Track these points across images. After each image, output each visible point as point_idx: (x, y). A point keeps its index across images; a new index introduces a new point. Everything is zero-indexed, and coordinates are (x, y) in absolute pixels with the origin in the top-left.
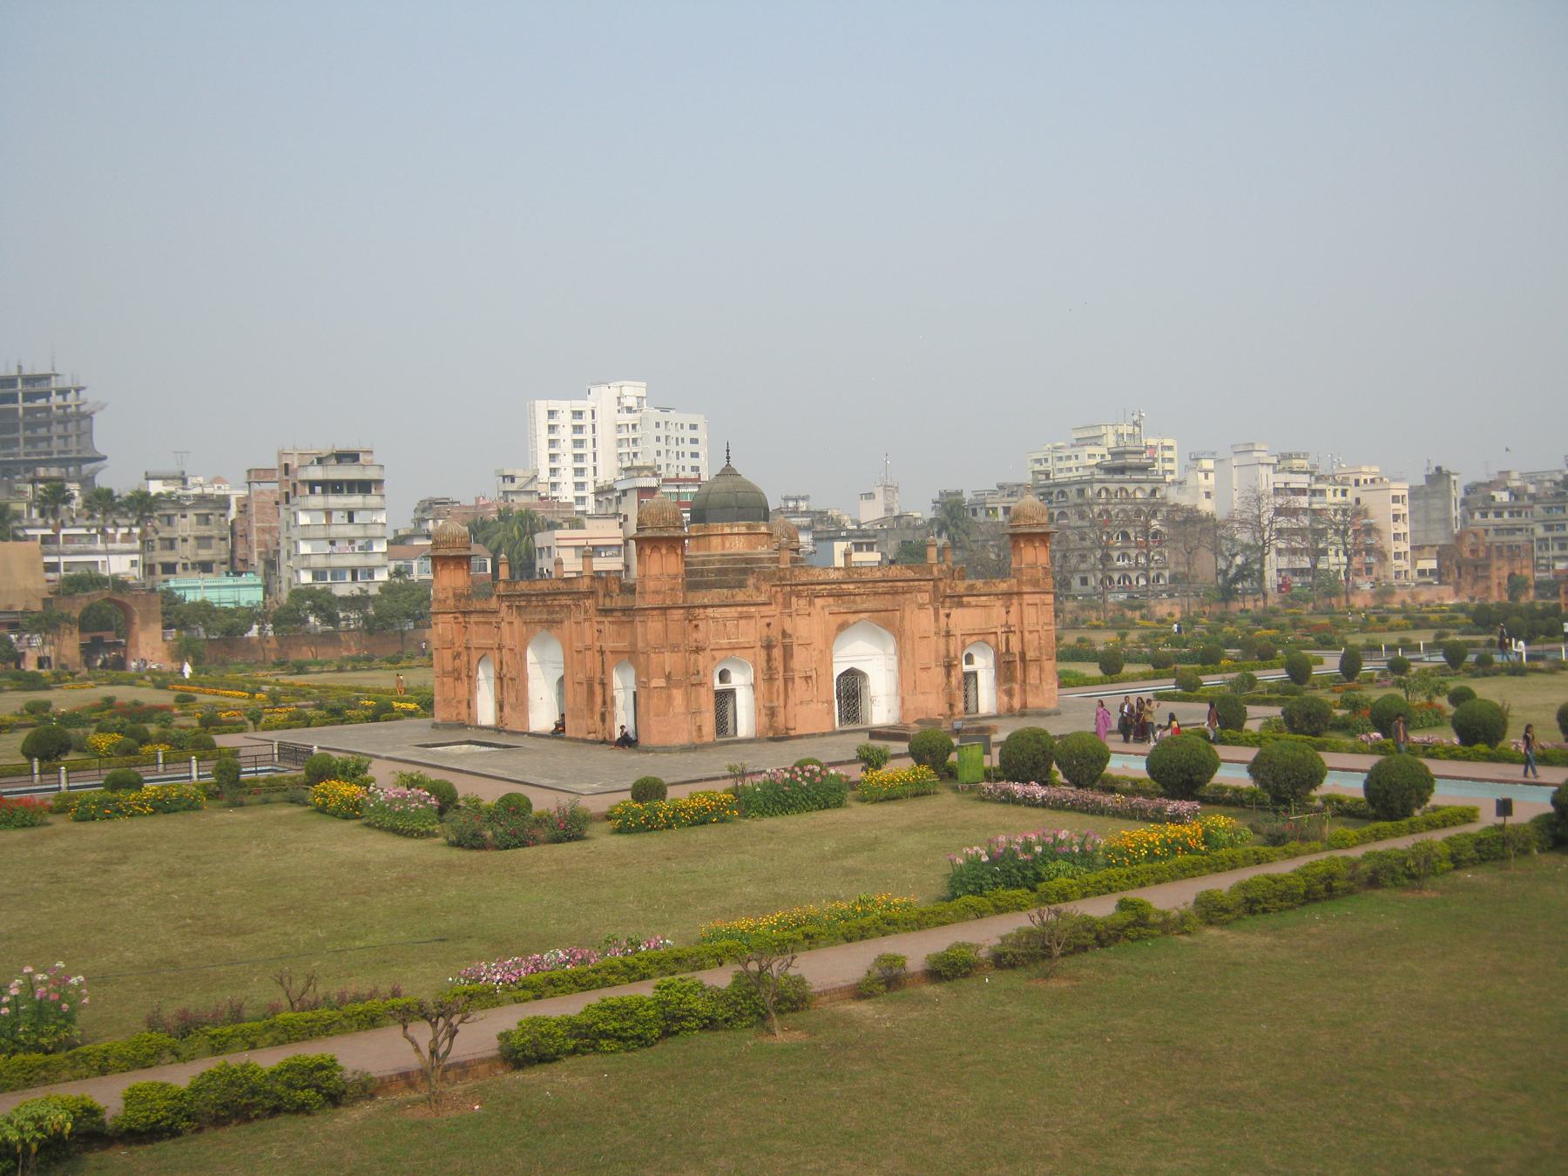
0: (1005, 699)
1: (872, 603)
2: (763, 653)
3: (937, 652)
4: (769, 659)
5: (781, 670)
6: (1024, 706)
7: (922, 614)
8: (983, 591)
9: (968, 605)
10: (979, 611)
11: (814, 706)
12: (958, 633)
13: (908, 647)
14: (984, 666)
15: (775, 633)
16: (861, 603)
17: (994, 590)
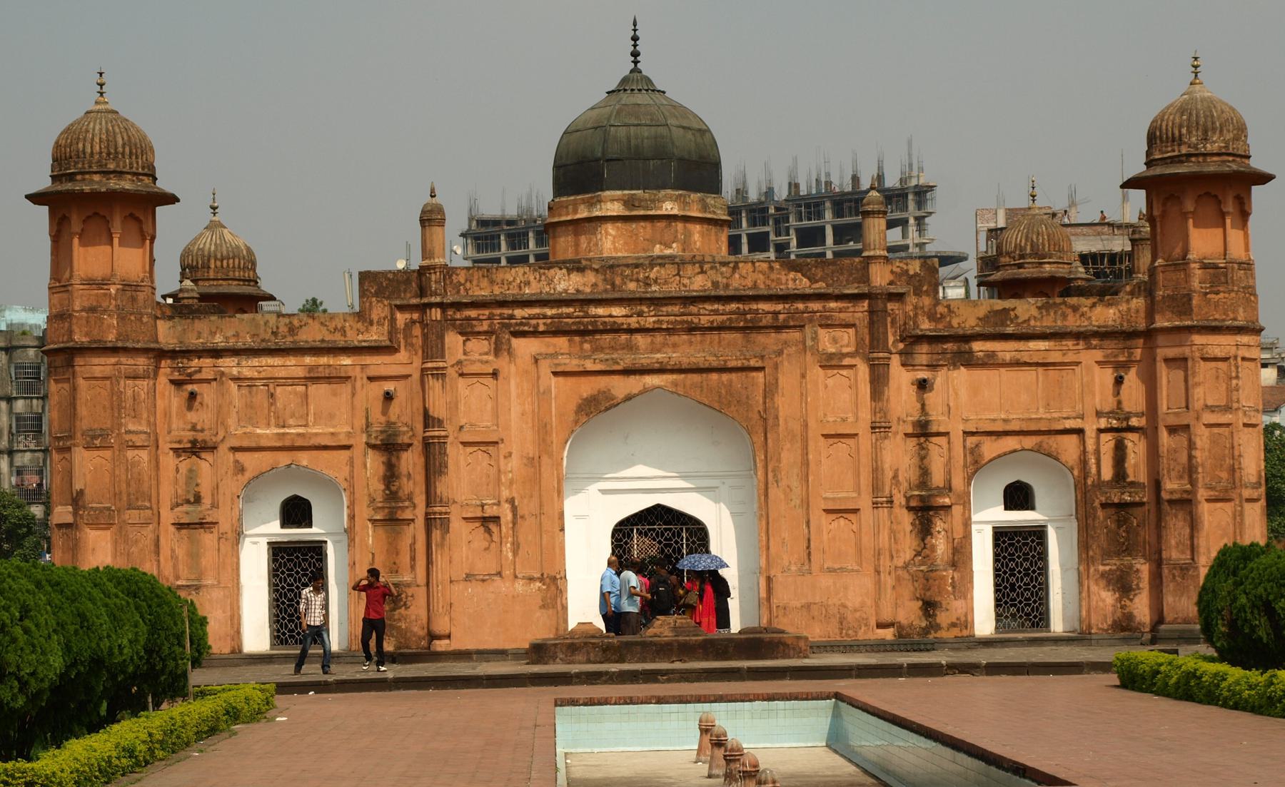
0: (1106, 598)
2: (374, 464)
3: (876, 471)
4: (391, 475)
5: (420, 500)
6: (1159, 619)
7: (836, 380)
8: (1037, 326)
9: (990, 362)
10: (1028, 375)
11: (501, 586)
12: (957, 429)
13: (789, 457)
15: (404, 413)
16: (645, 350)
17: (1073, 322)
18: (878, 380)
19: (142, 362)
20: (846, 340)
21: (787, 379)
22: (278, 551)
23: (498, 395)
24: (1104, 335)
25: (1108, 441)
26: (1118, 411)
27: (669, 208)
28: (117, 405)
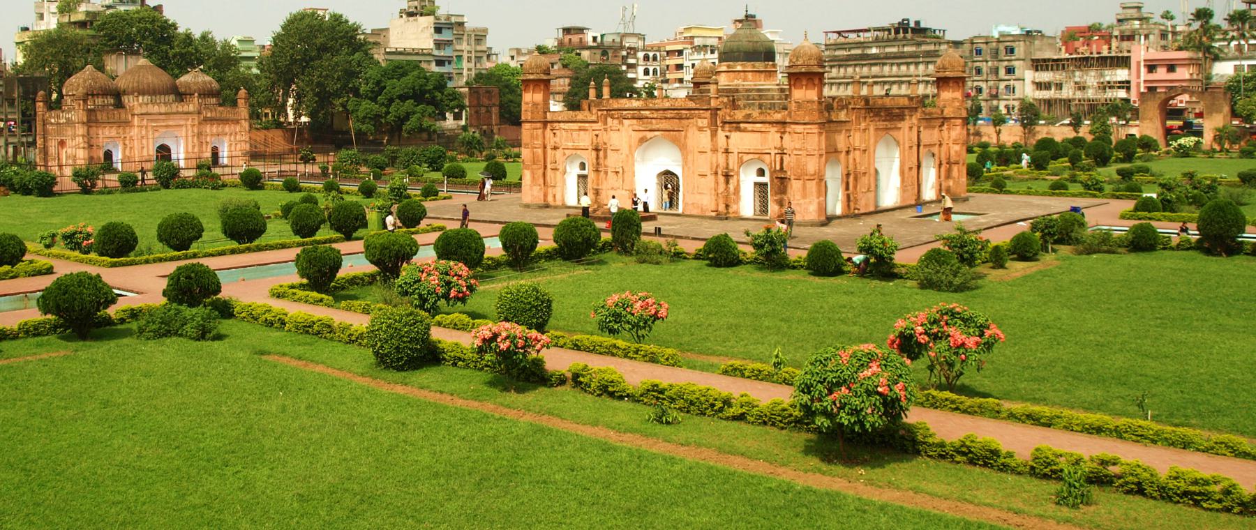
1: (665, 125)
2: (594, 153)
4: (598, 158)
7: (702, 135)
9: (745, 130)
13: (690, 158)
14: (748, 180)
16: (655, 124)
17: (768, 119)
18: (714, 134)
19: (539, 125)
20: (705, 121)
21: (690, 135)
22: (579, 176)
23: (621, 135)
24: (777, 123)
25: (778, 157)
26: (782, 148)
27: (739, 68)
28: (532, 137)
